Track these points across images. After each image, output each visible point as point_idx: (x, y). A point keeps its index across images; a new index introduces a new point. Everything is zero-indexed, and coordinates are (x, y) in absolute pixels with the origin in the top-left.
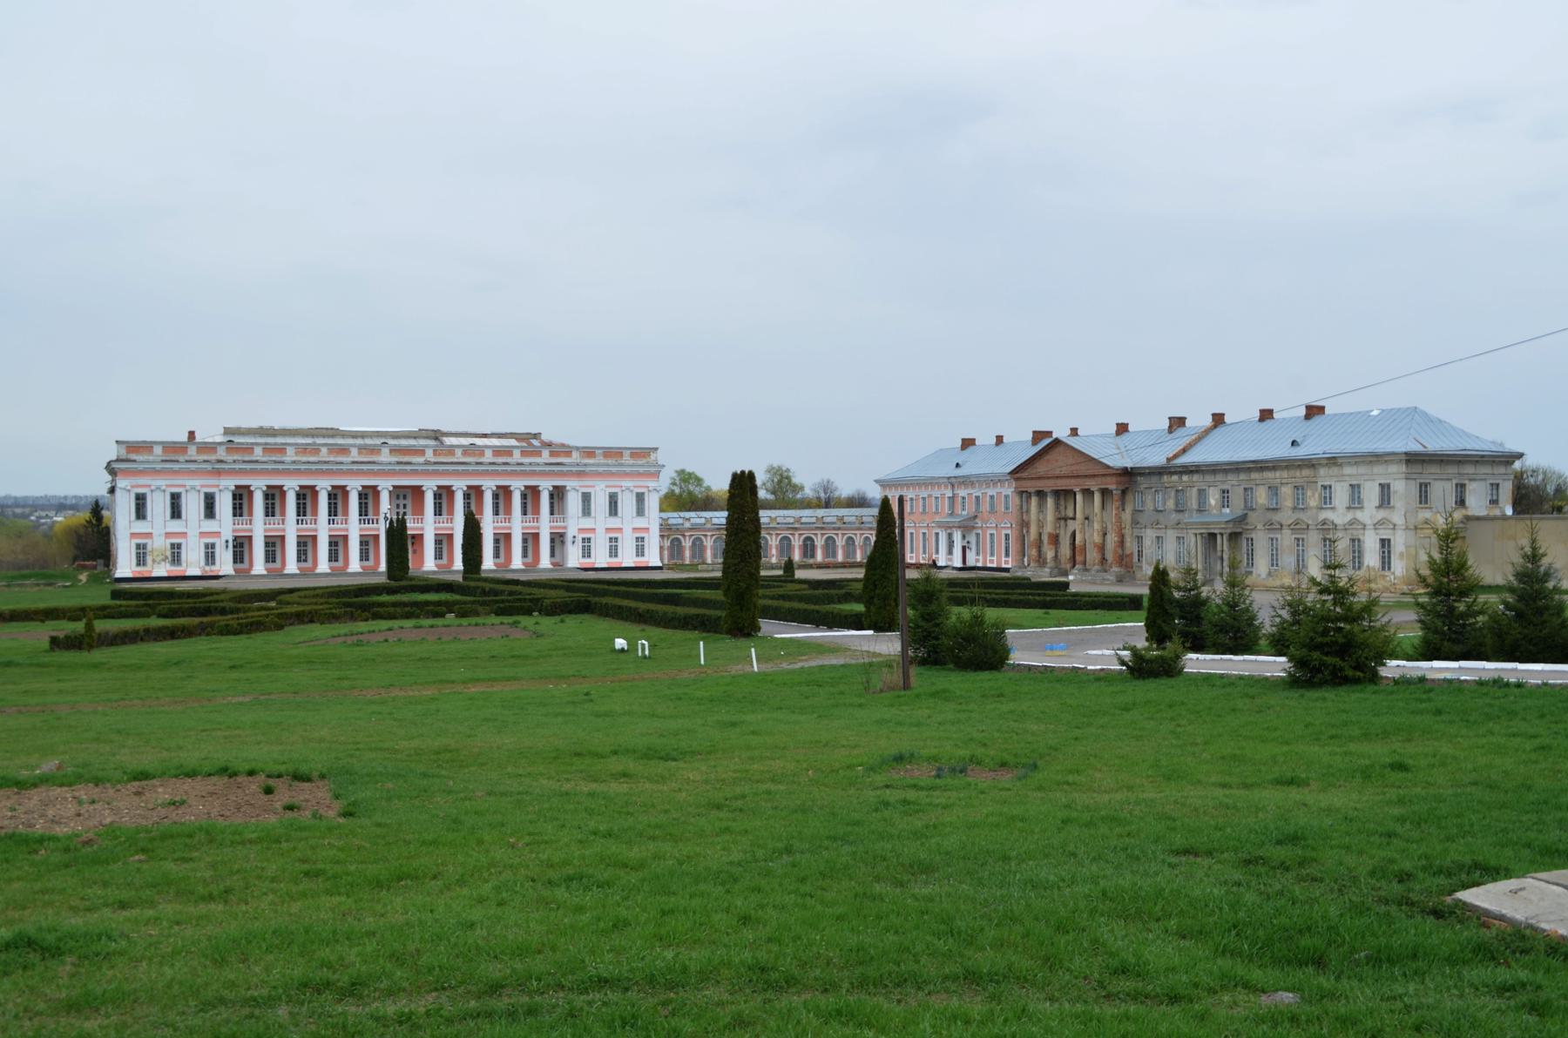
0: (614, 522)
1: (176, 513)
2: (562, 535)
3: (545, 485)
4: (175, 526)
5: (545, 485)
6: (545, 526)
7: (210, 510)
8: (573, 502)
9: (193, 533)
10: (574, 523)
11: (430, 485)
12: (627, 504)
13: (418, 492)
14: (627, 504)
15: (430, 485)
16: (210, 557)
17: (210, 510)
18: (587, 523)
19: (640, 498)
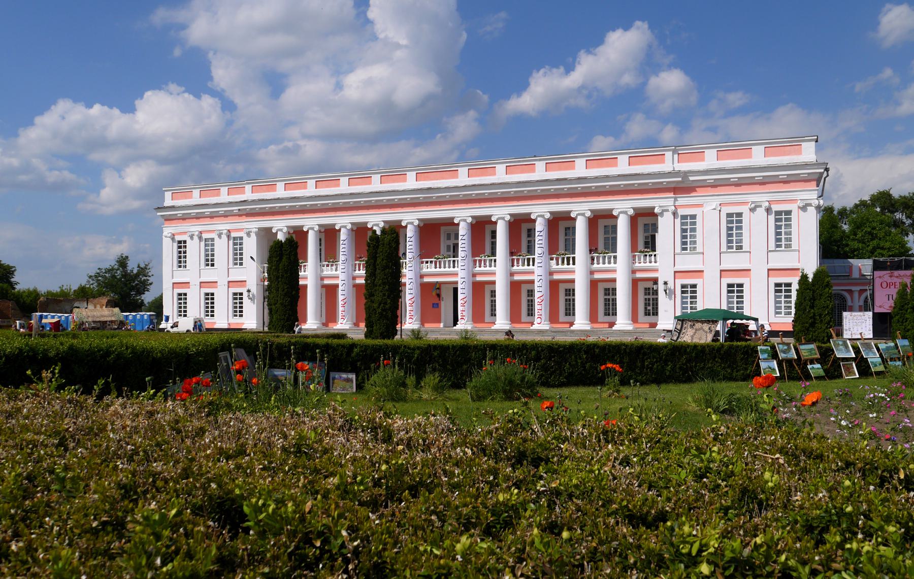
0: (733, 261)
1: (210, 262)
2: (655, 281)
3: (623, 208)
4: (209, 275)
5: (623, 208)
6: (620, 268)
7: (238, 259)
8: (667, 232)
9: (223, 282)
10: (665, 263)
11: (463, 215)
12: (758, 228)
13: (450, 224)
14: (758, 228)
15: (463, 215)
16: (238, 310)
17: (238, 259)
18: (688, 262)
19: (782, 218)
